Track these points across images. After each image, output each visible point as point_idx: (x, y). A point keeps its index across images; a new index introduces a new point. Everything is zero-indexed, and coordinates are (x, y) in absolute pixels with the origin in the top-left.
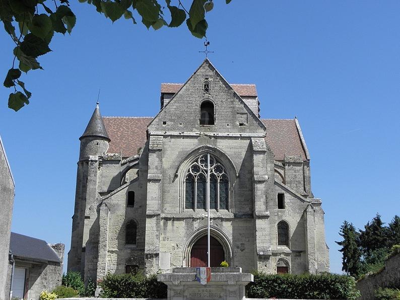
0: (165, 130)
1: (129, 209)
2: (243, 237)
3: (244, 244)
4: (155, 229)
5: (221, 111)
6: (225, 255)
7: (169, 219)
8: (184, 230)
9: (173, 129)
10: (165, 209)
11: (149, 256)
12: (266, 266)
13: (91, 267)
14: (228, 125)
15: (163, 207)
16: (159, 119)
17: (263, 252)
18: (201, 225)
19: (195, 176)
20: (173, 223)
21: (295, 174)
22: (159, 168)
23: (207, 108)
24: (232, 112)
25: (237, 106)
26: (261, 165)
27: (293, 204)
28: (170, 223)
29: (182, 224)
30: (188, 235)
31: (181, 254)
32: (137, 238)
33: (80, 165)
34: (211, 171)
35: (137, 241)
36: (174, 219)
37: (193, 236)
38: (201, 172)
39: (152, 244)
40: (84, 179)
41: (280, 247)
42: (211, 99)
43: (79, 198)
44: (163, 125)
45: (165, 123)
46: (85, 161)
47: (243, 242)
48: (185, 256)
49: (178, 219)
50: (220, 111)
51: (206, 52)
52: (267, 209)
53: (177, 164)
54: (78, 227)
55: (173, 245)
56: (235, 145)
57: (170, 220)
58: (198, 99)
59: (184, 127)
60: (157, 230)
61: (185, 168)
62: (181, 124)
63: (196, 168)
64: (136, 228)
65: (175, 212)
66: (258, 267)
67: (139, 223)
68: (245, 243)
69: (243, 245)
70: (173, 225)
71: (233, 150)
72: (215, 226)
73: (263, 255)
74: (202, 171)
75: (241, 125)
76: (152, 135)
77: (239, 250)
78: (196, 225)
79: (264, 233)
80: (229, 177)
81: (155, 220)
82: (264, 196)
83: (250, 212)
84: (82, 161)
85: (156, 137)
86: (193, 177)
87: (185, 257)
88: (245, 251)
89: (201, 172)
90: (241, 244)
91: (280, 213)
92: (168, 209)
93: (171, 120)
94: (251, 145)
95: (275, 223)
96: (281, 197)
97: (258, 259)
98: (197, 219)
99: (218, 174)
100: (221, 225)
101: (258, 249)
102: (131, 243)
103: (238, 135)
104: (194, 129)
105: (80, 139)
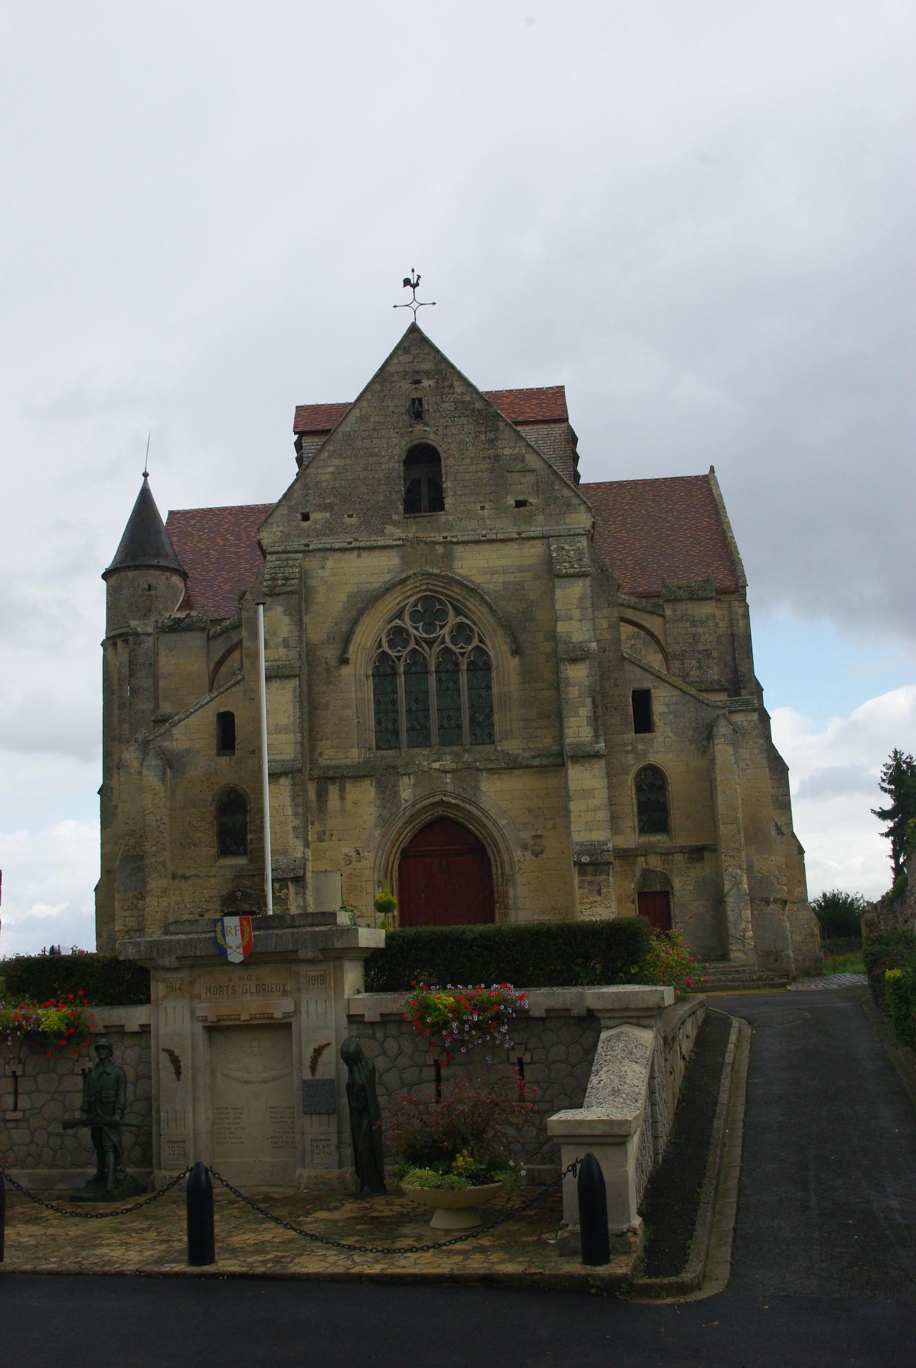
0: (308, 536)
1: (224, 760)
3: (541, 836)
4: (289, 811)
5: (461, 469)
6: (494, 870)
7: (333, 779)
8: (372, 809)
9: (330, 530)
10: (321, 754)
13: (132, 923)
14: (483, 508)
15: (312, 749)
16: (292, 509)
17: (591, 855)
19: (399, 658)
20: (342, 790)
21: (693, 630)
22: (293, 643)
23: (423, 461)
24: (492, 470)
25: (507, 452)
26: (576, 614)
27: (676, 716)
30: (384, 822)
32: (249, 837)
33: (110, 649)
34: (443, 642)
35: (249, 847)
38: (412, 645)
40: (121, 686)
41: (644, 839)
42: (432, 439)
43: (113, 739)
44: (305, 524)
45: (306, 517)
46: (120, 635)
47: (539, 833)
50: (460, 470)
51: (415, 305)
52: (596, 736)
53: (344, 629)
54: (114, 816)
55: (345, 850)
56: (503, 562)
58: (395, 441)
59: (361, 524)
61: (370, 633)
62: (350, 516)
63: (398, 635)
64: (245, 812)
65: (348, 762)
67: (252, 796)
70: (342, 798)
71: (500, 578)
74: (417, 643)
75: (520, 504)
76: (271, 553)
77: (528, 854)
80: (492, 654)
81: (288, 788)
82: (588, 701)
83: (555, 748)
84: (114, 637)
85: (284, 556)
86: (393, 662)
88: (543, 856)
89: (412, 645)
91: (640, 746)
92: (329, 753)
93: (322, 507)
94: (549, 562)
95: (627, 773)
96: (642, 699)
99: (462, 648)
100: (477, 788)
102: (234, 854)
103: (512, 533)
104: (389, 529)
105: (105, 576)
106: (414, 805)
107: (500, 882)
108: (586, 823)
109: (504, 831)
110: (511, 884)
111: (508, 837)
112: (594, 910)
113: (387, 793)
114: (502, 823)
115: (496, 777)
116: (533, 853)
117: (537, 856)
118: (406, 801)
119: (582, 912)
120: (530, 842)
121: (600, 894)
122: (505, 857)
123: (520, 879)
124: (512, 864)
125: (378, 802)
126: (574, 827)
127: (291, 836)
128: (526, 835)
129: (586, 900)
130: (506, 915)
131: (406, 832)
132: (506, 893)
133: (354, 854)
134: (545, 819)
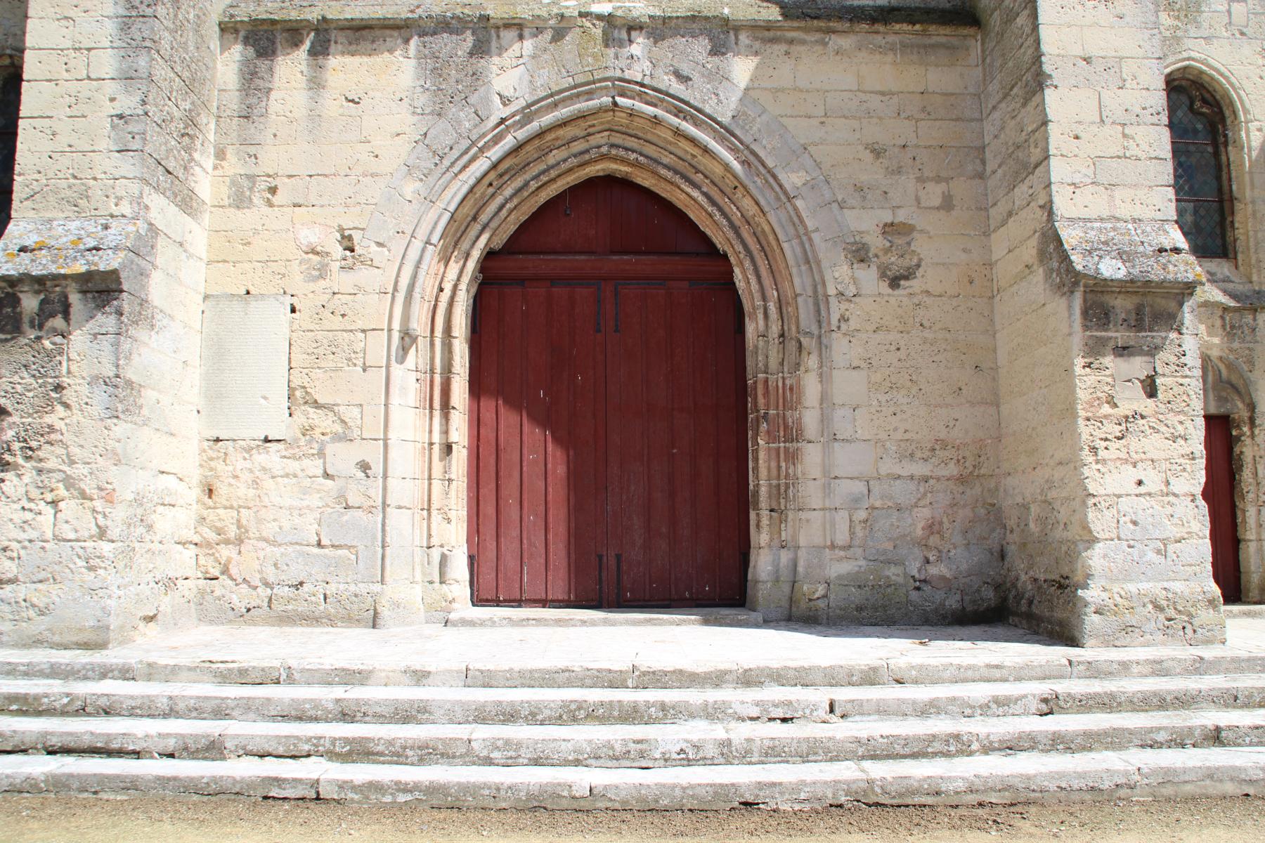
2: (899, 171)
4: (106, 63)
6: (751, 329)
7: (293, 33)
8: (405, 121)
11: (30, 303)
12: (1151, 391)
18: (550, 79)
28: (291, 67)
29: (394, 74)
31: (375, 310)
36: (324, 37)
37: (481, 165)
39: (76, 203)
47: (901, 216)
48: (419, 325)
49: (365, 34)
55: (310, 236)
57: (296, 44)
60: (128, 78)
66: (1082, 395)
68: (918, 220)
69: (899, 241)
70: (316, 84)
72: (668, 82)
73: (1128, 287)
77: (868, 277)
78: (513, 77)
79: (1115, 101)
87: (408, 338)
88: (915, 285)
90: (889, 229)
97: (1078, 337)
98: (518, 27)
101: (1070, 236)
106: (527, 114)
107: (773, 363)
108: (1096, 160)
109: (799, 203)
110: (812, 362)
111: (810, 224)
112: (1133, 442)
113: (448, 91)
114: (792, 179)
115: (783, 47)
116: (883, 275)
117: (895, 282)
118: (505, 101)
119: (1094, 450)
120: (876, 242)
121: (1151, 391)
122: (800, 281)
123: (842, 350)
124: (820, 302)
125: (422, 100)
126: (1058, 170)
127: (103, 144)
128: (865, 223)
129: (1106, 409)
130: (793, 457)
131: (499, 200)
132: (791, 397)
133: (338, 251)
134: (921, 180)
